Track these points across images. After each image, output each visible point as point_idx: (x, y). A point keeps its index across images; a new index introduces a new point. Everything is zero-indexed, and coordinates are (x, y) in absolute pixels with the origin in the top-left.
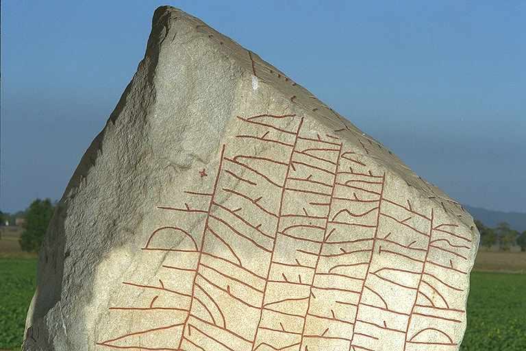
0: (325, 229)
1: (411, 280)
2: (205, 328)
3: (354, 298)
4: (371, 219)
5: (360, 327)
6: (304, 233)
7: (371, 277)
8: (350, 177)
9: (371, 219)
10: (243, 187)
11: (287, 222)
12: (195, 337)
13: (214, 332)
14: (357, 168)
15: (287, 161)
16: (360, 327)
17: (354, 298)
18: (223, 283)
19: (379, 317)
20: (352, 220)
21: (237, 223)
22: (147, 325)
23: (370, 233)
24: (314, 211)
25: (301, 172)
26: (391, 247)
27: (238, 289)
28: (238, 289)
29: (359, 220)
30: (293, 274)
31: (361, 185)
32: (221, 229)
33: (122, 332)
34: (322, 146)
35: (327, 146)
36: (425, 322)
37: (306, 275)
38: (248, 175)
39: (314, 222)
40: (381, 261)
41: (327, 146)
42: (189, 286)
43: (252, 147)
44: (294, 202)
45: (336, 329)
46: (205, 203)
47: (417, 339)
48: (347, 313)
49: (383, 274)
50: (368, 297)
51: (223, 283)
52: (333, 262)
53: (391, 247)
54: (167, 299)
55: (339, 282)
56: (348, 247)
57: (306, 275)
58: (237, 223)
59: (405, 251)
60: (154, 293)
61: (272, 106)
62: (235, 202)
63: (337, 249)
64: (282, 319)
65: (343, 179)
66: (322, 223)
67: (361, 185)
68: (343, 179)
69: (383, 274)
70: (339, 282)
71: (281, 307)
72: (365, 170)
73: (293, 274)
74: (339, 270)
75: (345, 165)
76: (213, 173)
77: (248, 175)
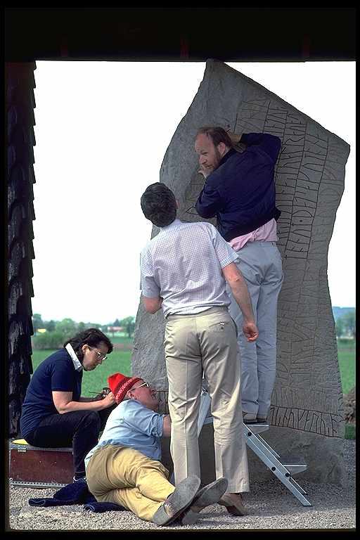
3: (295, 177)
5: (298, 189)
8: (292, 125)
14: (294, 121)
16: (298, 189)
17: (295, 177)
19: (306, 184)
23: (301, 148)
26: (311, 154)
34: (279, 112)
35: (282, 112)
40: (305, 160)
41: (282, 112)
53: (311, 154)
59: (317, 156)
69: (307, 166)
72: (298, 122)
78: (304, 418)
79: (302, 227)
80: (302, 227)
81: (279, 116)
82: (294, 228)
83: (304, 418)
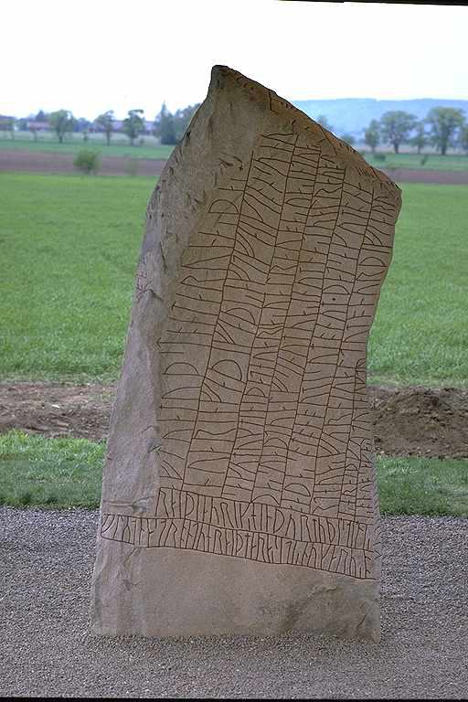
0: (311, 200)
1: (360, 230)
2: (244, 258)
4: (338, 194)
6: (298, 202)
7: (338, 230)
8: (325, 170)
9: (338, 194)
10: (263, 176)
11: (288, 197)
12: (237, 262)
13: (248, 260)
15: (289, 161)
18: (253, 232)
20: (327, 195)
21: (260, 197)
22: (210, 255)
24: (304, 190)
25: (296, 167)
27: (261, 236)
28: (261, 236)
29: (331, 195)
30: (293, 226)
31: (329, 174)
32: (251, 201)
33: (196, 260)
36: (368, 254)
37: (301, 227)
38: (267, 169)
39: (304, 196)
42: (233, 234)
43: (268, 153)
44: (294, 185)
45: (316, 258)
46: (241, 186)
47: (363, 263)
48: (324, 249)
49: (345, 226)
50: (336, 239)
51: (253, 232)
52: (316, 219)
54: (221, 241)
55: (319, 231)
56: (324, 211)
57: (301, 227)
58: (260, 197)
59: (357, 213)
60: (213, 238)
61: (280, 129)
62: (258, 185)
63: (318, 212)
64: (287, 252)
65: (321, 171)
66: (309, 197)
67: (335, 175)
68: (321, 171)
69: (345, 226)
70: (319, 231)
71: (284, 245)
73: (293, 226)
74: (321, 224)
75: (322, 163)
76: (246, 169)
77: (267, 169)
78: (329, 555)
79: (333, 308)
80: (333, 308)
81: (312, 157)
82: (323, 309)
83: (329, 555)
